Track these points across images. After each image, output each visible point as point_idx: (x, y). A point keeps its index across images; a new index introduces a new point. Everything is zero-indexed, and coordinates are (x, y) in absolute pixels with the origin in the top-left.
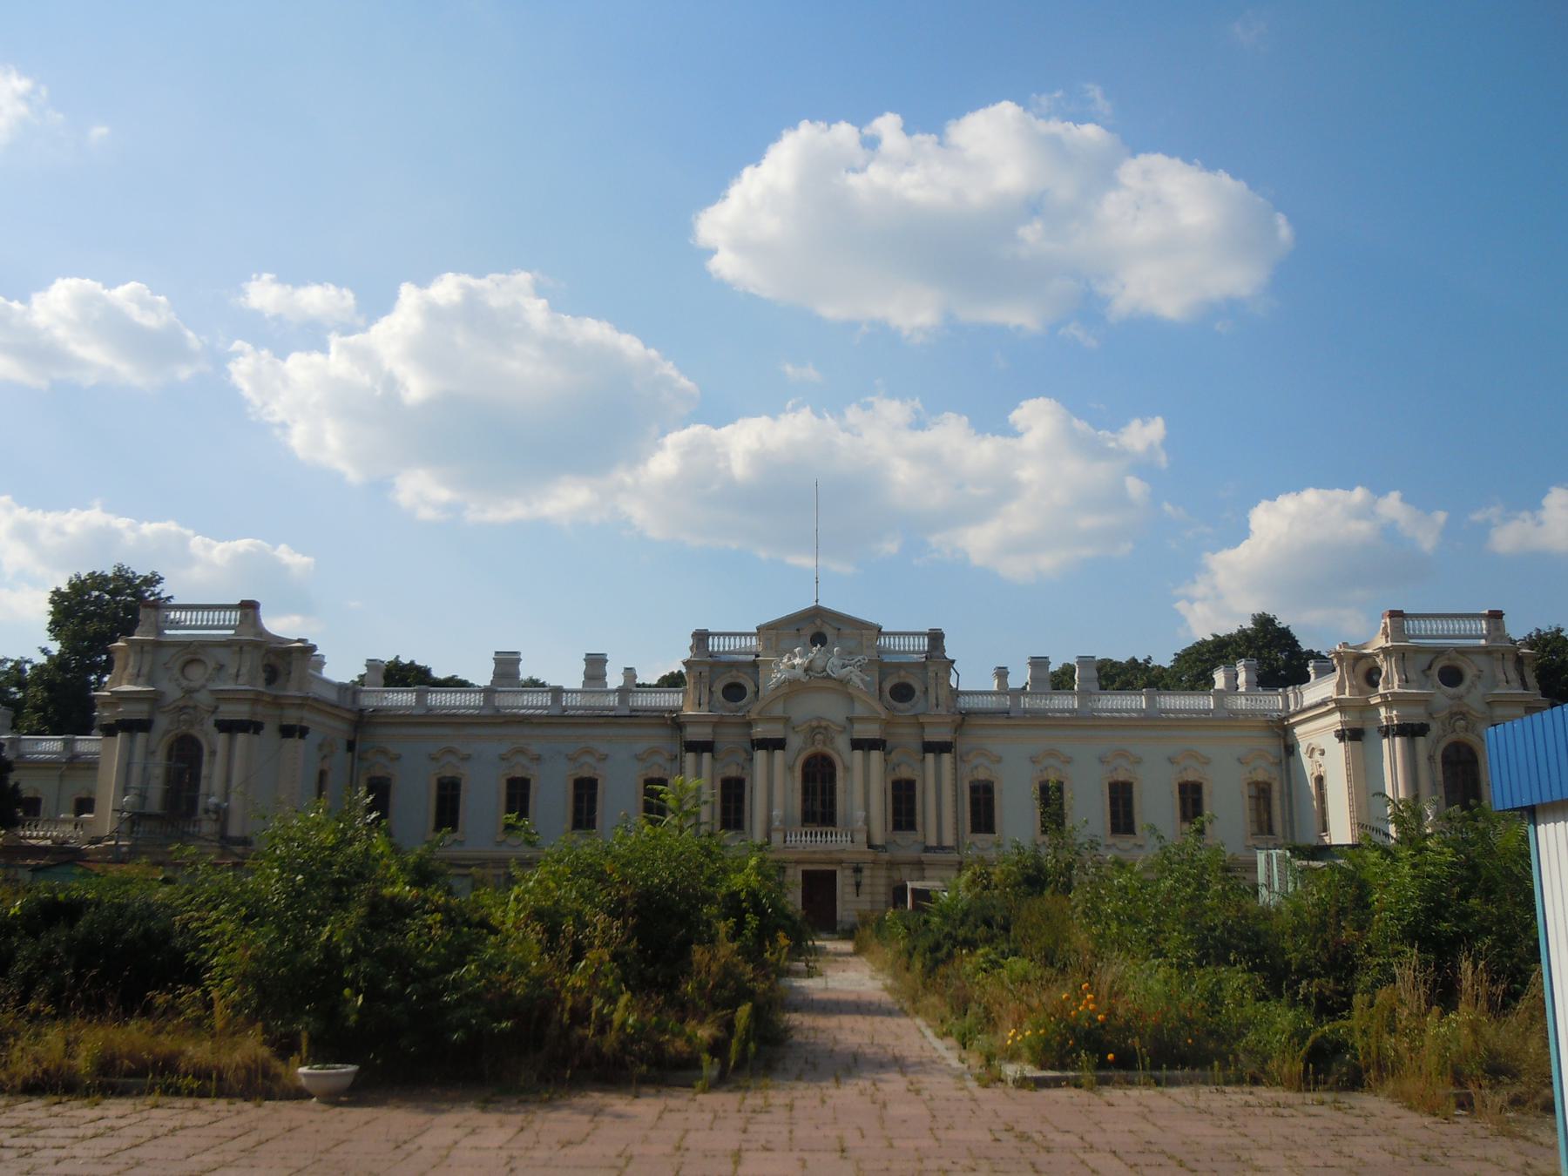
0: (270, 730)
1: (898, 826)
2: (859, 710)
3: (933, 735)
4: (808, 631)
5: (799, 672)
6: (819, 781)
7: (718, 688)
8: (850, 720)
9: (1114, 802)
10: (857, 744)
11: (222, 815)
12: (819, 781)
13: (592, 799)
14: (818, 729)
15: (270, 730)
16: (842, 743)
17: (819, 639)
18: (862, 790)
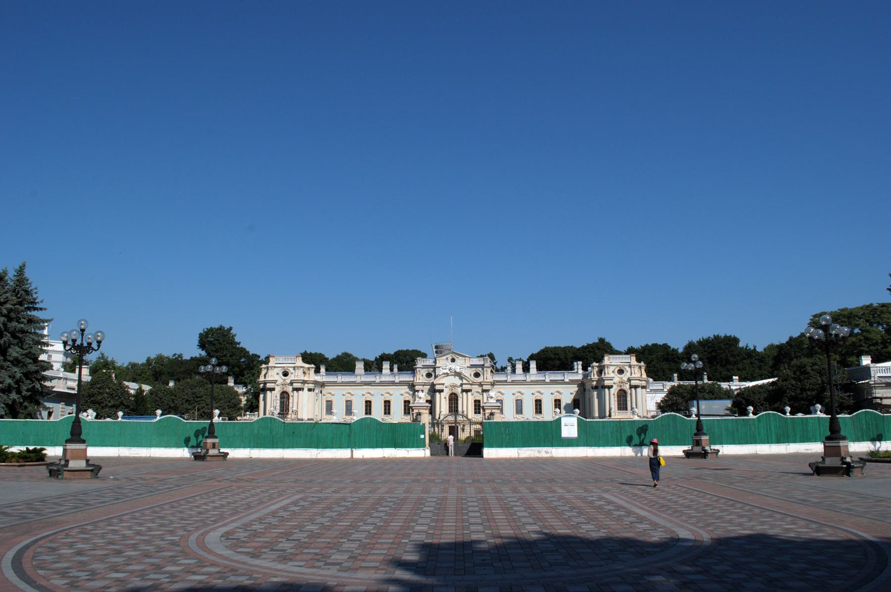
0: (306, 389)
1: (475, 413)
2: (465, 381)
3: (485, 387)
4: (450, 358)
5: (447, 371)
6: (453, 399)
7: (424, 375)
8: (462, 385)
9: (536, 405)
10: (463, 391)
11: (296, 412)
12: (453, 399)
13: (389, 406)
14: (454, 386)
15: (306, 389)
16: (459, 390)
17: (453, 360)
18: (466, 404)
